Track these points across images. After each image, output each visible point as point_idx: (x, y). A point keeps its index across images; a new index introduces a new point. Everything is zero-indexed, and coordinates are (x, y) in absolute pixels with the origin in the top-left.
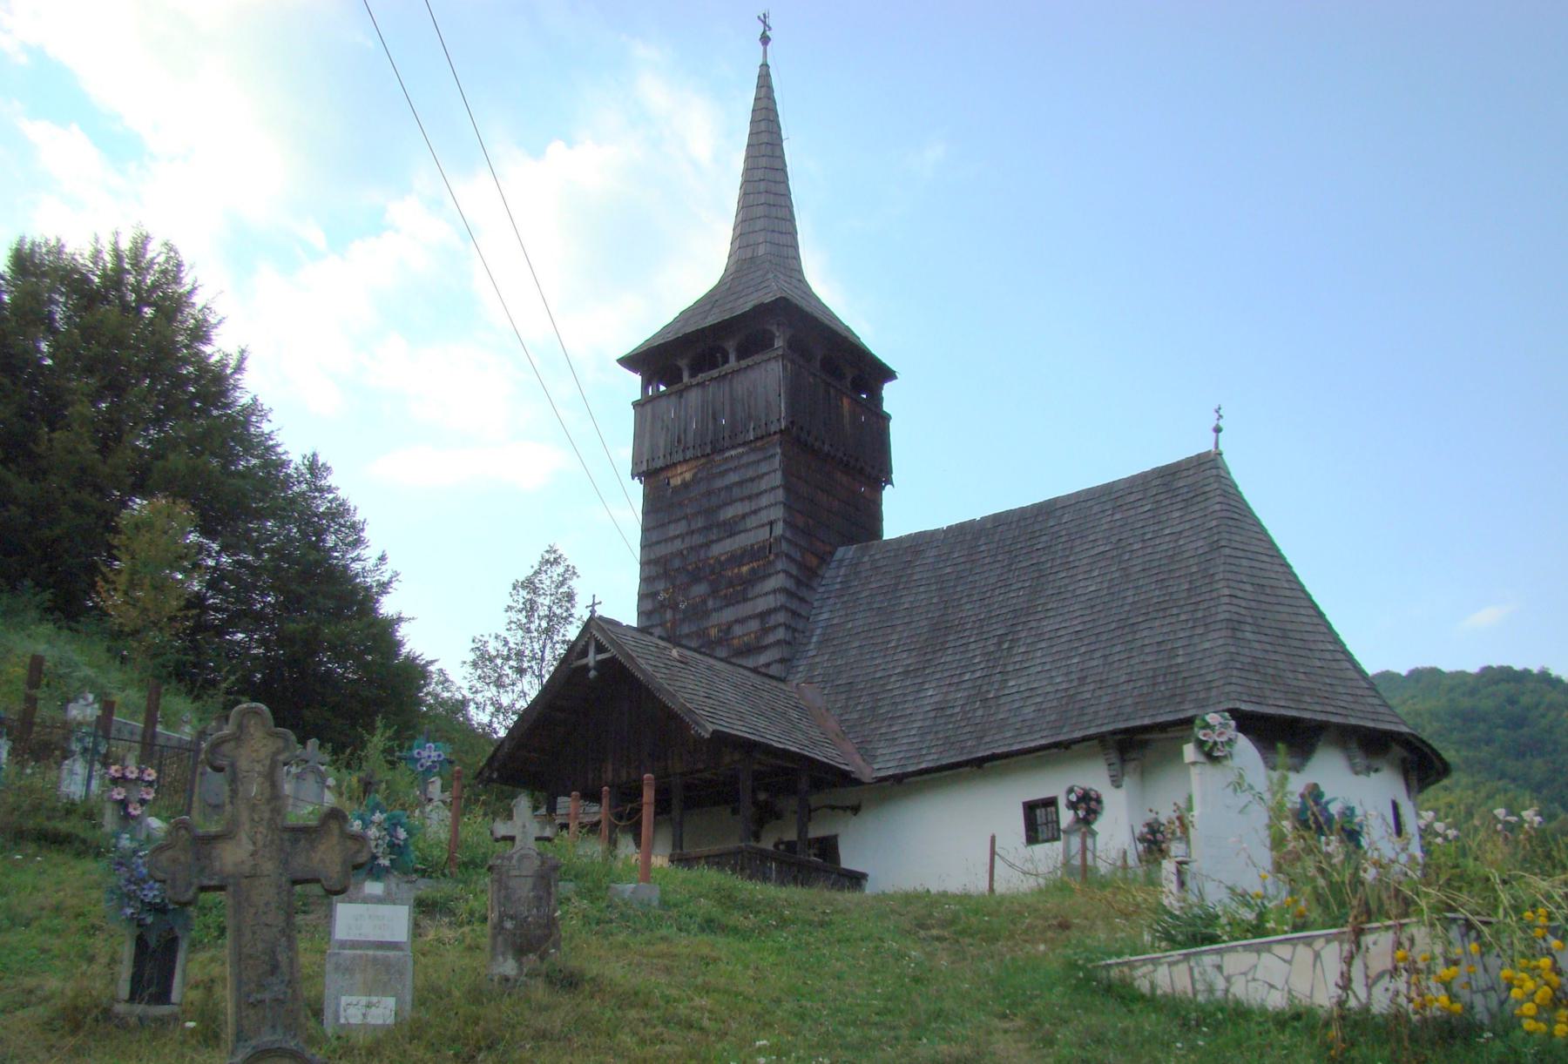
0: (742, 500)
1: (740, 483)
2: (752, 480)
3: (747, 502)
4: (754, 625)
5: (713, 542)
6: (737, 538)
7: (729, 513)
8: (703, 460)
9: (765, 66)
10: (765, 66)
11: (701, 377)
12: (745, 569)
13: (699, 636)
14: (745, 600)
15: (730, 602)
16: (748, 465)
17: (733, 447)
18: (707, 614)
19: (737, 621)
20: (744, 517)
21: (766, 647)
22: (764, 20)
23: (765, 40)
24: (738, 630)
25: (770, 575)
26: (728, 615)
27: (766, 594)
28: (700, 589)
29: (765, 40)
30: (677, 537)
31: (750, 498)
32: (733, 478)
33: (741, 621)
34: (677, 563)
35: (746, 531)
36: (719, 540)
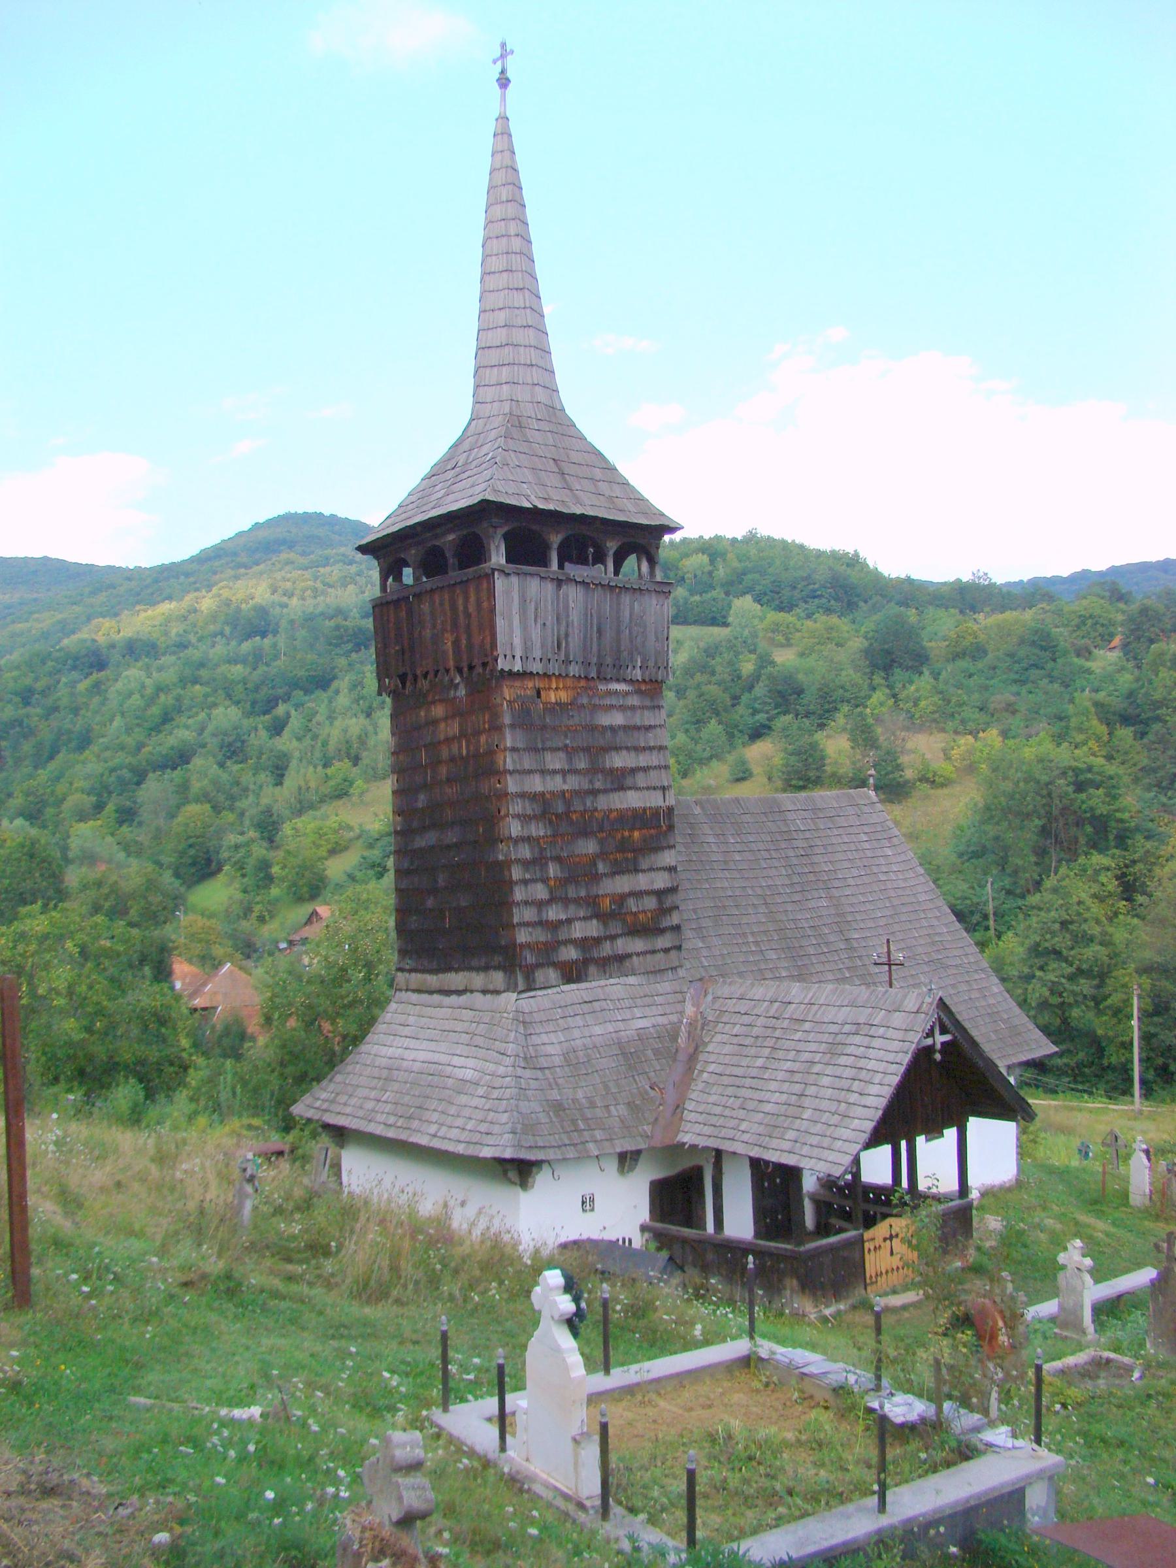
0: (627, 748)
1: (625, 728)
2: (637, 728)
3: (633, 754)
4: (650, 903)
5: (599, 791)
6: (630, 793)
7: (618, 760)
8: (583, 683)
9: (503, 119)
10: (503, 119)
11: (572, 570)
12: (636, 834)
13: (588, 904)
14: (637, 871)
15: (618, 870)
16: (633, 708)
17: (618, 680)
18: (596, 878)
19: (632, 894)
20: (634, 771)
21: (662, 931)
22: (505, 52)
23: (504, 82)
24: (632, 905)
25: (662, 849)
26: (622, 884)
27: (664, 869)
28: (589, 847)
29: (504, 82)
30: (555, 772)
31: (637, 749)
32: (618, 719)
33: (638, 894)
34: (561, 809)
35: (637, 789)
36: (605, 791)
